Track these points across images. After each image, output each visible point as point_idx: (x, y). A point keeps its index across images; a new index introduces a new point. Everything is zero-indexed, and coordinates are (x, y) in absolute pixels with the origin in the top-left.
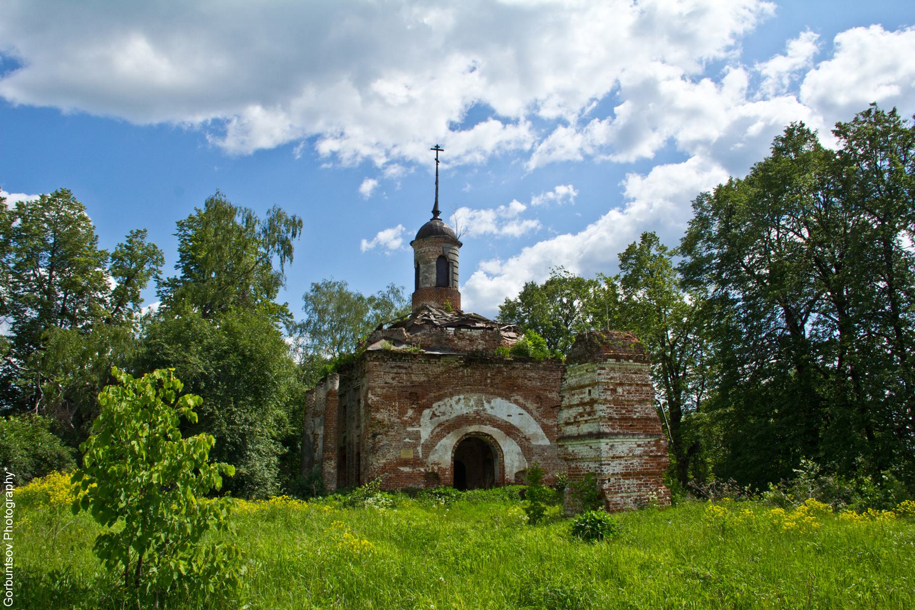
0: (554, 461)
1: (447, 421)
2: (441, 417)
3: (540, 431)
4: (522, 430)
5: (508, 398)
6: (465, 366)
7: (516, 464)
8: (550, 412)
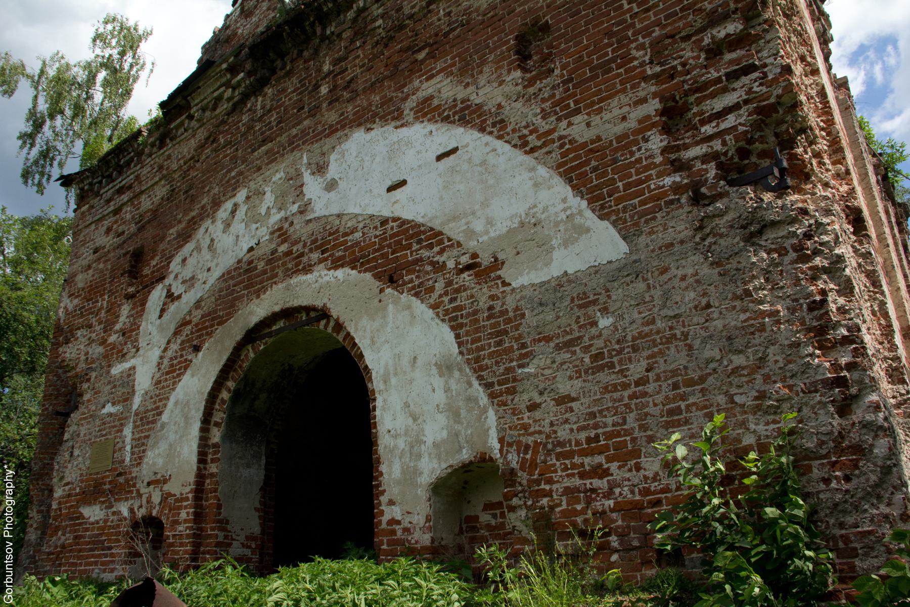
0: (676, 358)
1: (198, 304)
2: (185, 298)
3: (558, 196)
4: (454, 231)
5: (391, 114)
6: (256, 89)
7: (435, 429)
8: (605, 68)
